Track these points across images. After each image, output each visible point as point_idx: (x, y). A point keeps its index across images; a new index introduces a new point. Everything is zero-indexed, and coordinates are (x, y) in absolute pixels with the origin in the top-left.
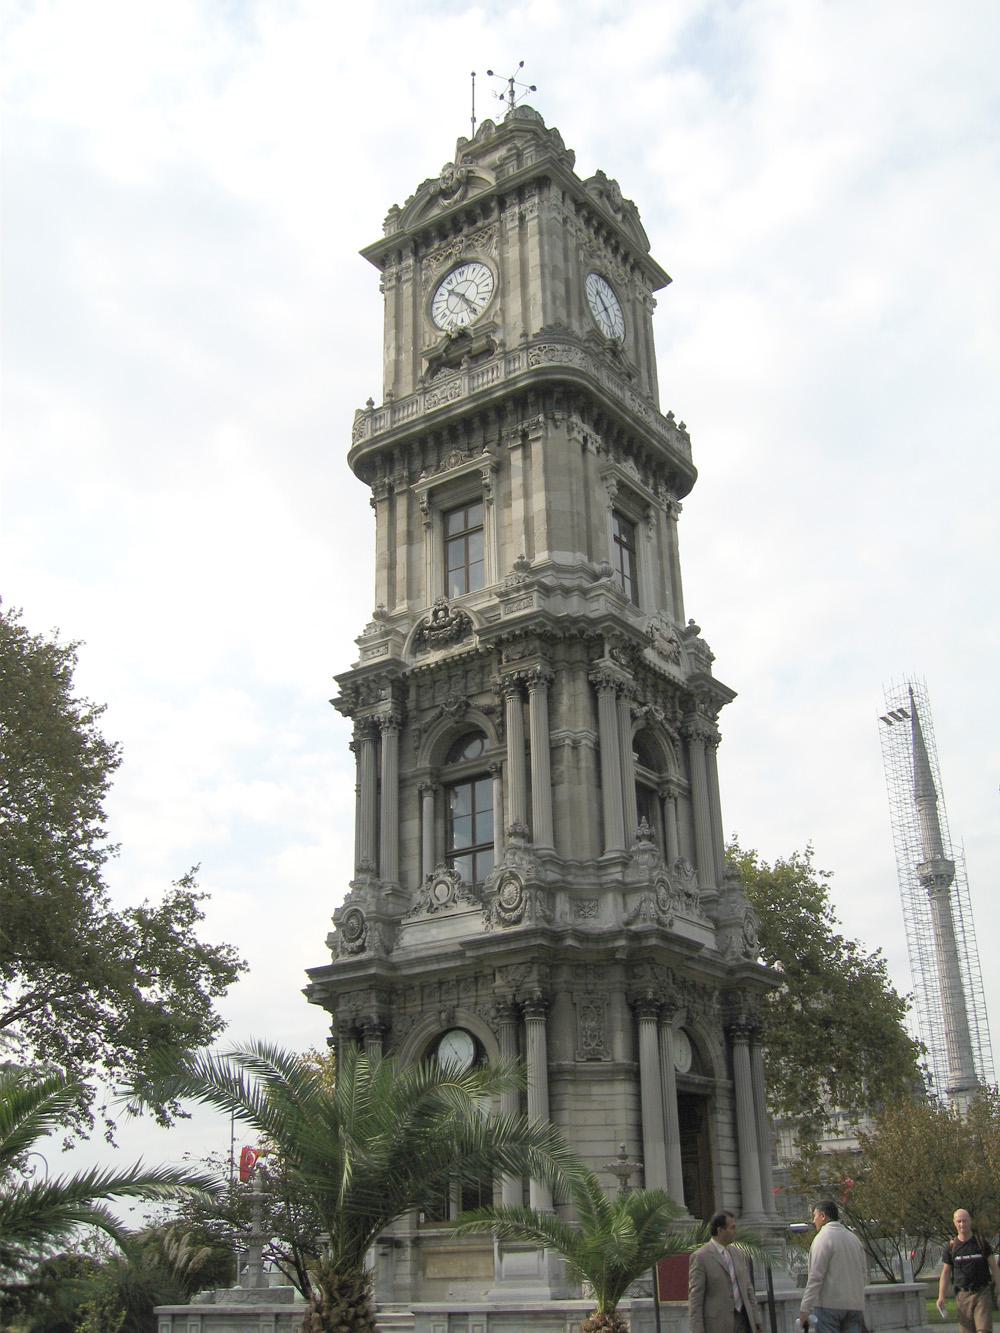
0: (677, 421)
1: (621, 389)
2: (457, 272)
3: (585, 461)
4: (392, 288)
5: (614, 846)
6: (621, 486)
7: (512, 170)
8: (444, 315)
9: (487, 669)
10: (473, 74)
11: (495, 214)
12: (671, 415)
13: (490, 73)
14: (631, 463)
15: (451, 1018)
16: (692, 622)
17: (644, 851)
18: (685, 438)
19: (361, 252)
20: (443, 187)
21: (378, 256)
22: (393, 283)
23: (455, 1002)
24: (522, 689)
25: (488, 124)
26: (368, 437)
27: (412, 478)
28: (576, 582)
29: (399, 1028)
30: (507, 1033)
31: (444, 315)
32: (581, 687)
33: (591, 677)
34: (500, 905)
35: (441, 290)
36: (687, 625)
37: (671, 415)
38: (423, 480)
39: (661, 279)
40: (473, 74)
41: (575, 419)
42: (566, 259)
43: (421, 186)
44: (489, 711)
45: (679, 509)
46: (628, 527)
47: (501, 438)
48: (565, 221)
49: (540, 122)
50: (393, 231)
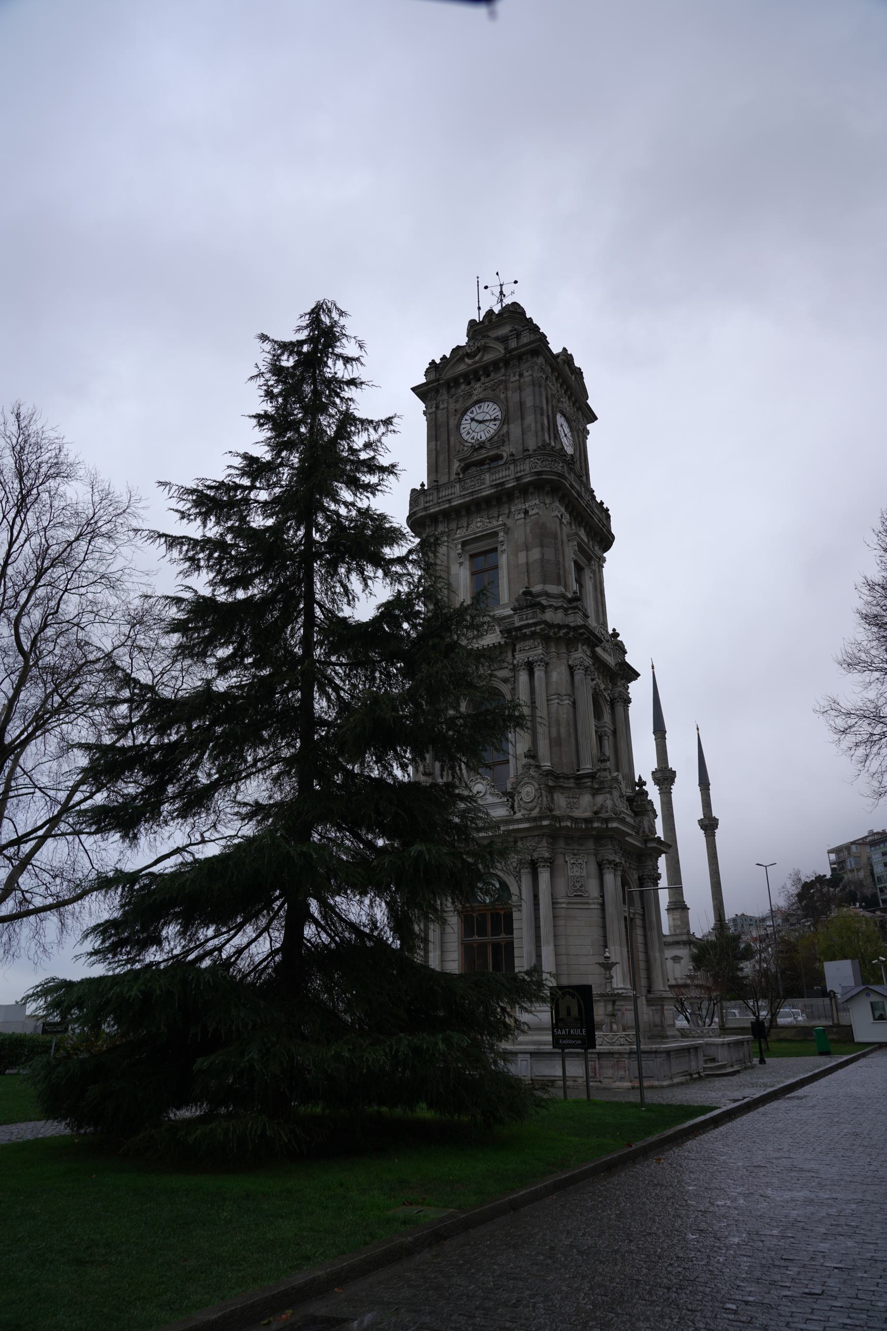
0: (605, 506)
2: (477, 406)
6: (579, 545)
7: (513, 344)
8: (469, 433)
10: (478, 277)
11: (503, 370)
12: (602, 503)
14: (583, 530)
16: (614, 630)
19: (413, 389)
22: (434, 409)
24: (530, 667)
25: (490, 312)
26: (422, 506)
28: (560, 604)
30: (526, 880)
31: (469, 433)
32: (564, 669)
33: (570, 662)
34: (521, 799)
35: (466, 417)
38: (458, 536)
39: (593, 418)
40: (478, 277)
41: (557, 504)
44: (505, 681)
45: (604, 560)
46: (579, 569)
47: (510, 512)
49: (523, 313)
50: (432, 376)
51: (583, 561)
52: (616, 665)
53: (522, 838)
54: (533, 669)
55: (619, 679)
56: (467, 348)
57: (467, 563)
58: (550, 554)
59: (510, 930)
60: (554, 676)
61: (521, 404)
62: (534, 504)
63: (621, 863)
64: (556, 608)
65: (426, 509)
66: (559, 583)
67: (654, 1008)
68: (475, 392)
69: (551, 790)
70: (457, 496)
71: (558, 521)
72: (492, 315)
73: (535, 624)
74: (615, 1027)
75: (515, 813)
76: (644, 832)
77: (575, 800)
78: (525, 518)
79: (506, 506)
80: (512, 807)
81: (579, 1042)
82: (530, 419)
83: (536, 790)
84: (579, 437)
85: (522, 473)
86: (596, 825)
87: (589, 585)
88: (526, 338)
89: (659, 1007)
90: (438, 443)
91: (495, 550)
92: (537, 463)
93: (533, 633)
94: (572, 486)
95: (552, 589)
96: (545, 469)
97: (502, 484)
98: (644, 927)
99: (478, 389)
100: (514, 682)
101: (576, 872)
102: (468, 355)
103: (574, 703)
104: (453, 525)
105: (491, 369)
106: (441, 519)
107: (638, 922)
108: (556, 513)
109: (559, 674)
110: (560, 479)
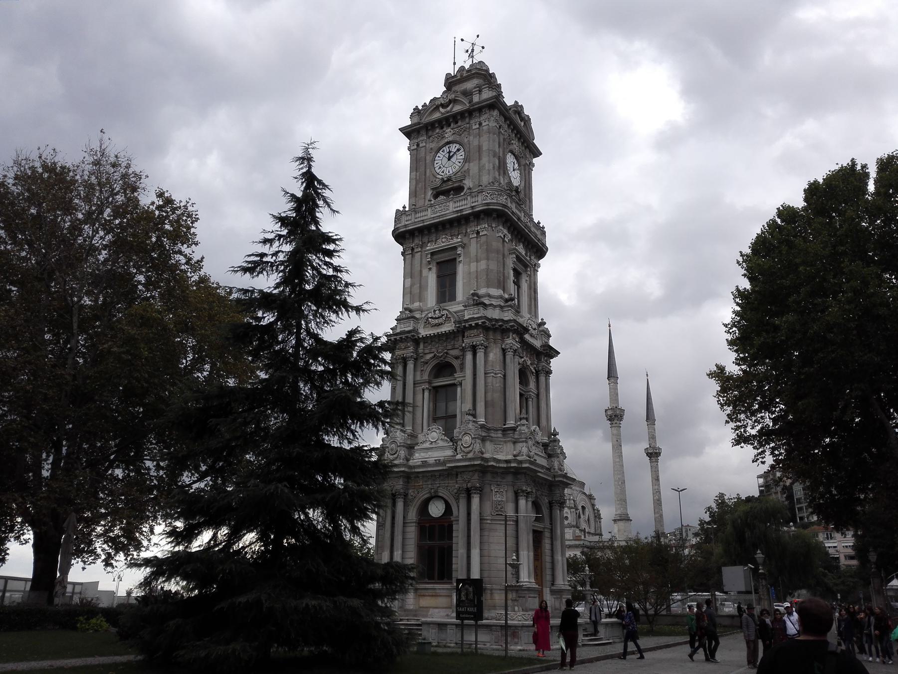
1: (520, 212)
2: (447, 147)
3: (504, 246)
4: (414, 151)
5: (511, 423)
6: (518, 258)
7: (476, 99)
8: (440, 168)
9: (457, 339)
10: (455, 38)
11: (467, 120)
12: (539, 223)
13: (462, 40)
15: (436, 492)
16: (542, 319)
17: (524, 425)
18: (544, 233)
19: (401, 130)
20: (443, 102)
21: (408, 132)
22: (415, 147)
23: (438, 485)
25: (462, 68)
26: (403, 224)
27: (422, 246)
28: (498, 303)
29: (412, 494)
31: (440, 168)
33: (503, 346)
34: (462, 444)
36: (540, 321)
37: (539, 223)
38: (428, 248)
39: (536, 153)
40: (455, 38)
42: (499, 147)
43: (431, 100)
44: (457, 358)
45: (539, 266)
46: (517, 274)
48: (500, 127)
49: (487, 70)
50: (416, 120)
51: (520, 268)
52: (541, 347)
53: (461, 473)
54: (476, 350)
55: (543, 356)
56: (442, 99)
57: (434, 269)
58: (493, 266)
59: (450, 537)
60: (491, 356)
61: (480, 148)
62: (484, 227)
63: (532, 492)
64: (495, 306)
65: (406, 226)
66: (498, 288)
67: (555, 596)
68: (446, 136)
69: (483, 440)
70: (429, 216)
71: (502, 240)
72: (463, 70)
73: (478, 318)
74: (516, 608)
75: (457, 454)
76: (554, 469)
77: (501, 446)
78: (477, 237)
79: (464, 227)
80: (456, 450)
81: (472, 616)
82: (485, 160)
83: (472, 438)
84: (525, 170)
85: (476, 203)
86: (513, 465)
87: (524, 286)
88: (487, 94)
89: (559, 596)
90: (418, 174)
91: (455, 259)
92: (487, 196)
93: (477, 324)
94: (513, 213)
95: (495, 292)
96: (493, 201)
97: (461, 211)
98: (552, 538)
99: (449, 134)
100: (463, 359)
101: (497, 498)
102: (443, 106)
103: (505, 376)
104: (425, 239)
105: (459, 117)
106: (417, 234)
107: (547, 534)
108: (500, 234)
109: (495, 355)
110: (504, 209)
